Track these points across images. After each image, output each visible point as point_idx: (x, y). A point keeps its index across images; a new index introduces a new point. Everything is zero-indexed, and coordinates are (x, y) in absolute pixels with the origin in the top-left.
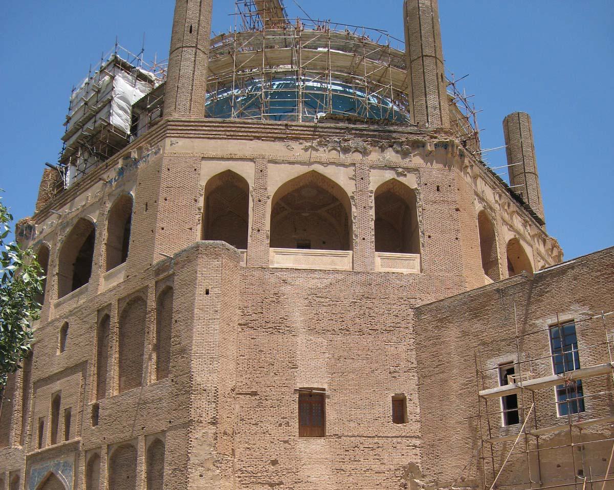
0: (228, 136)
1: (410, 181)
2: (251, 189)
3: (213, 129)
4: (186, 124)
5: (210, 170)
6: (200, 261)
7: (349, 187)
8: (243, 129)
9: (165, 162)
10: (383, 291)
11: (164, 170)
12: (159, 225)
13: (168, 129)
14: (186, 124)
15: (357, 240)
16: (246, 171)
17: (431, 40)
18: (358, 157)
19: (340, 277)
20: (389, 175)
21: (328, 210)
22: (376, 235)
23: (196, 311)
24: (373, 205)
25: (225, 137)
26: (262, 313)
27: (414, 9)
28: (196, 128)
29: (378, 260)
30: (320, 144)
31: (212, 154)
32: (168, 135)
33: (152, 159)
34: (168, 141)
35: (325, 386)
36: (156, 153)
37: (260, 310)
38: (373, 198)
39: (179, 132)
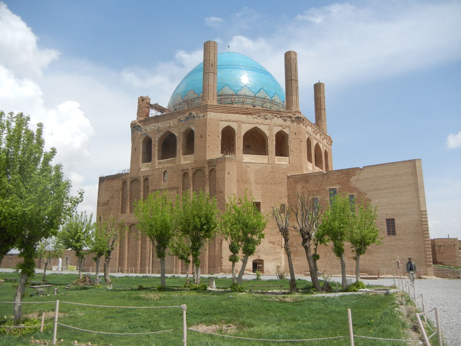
1: (286, 131)
6: (226, 163)
7: (267, 133)
9: (208, 122)
11: (208, 124)
12: (207, 145)
15: (270, 152)
16: (234, 126)
17: (295, 73)
19: (264, 165)
20: (280, 129)
23: (226, 180)
24: (275, 140)
29: (276, 159)
30: (258, 116)
31: (223, 119)
34: (208, 113)
35: (261, 201)
36: (204, 116)
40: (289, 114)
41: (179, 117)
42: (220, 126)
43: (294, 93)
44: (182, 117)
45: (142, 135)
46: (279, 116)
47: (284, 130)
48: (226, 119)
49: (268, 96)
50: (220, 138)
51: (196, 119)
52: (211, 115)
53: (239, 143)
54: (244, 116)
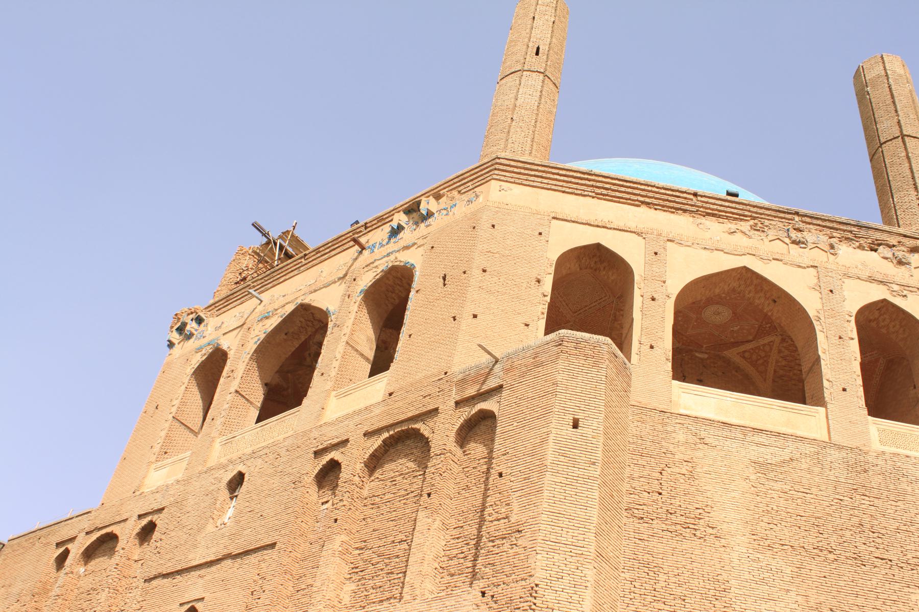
0: (597, 194)
2: (637, 278)
3: (573, 180)
4: (528, 166)
7: (810, 302)
8: (623, 189)
10: (892, 487)
13: (496, 169)
14: (528, 166)
15: (830, 390)
18: (818, 256)
19: (808, 449)
20: (876, 294)
21: (744, 352)
22: (864, 386)
25: (593, 194)
26: (660, 494)
27: (879, 76)
28: (544, 175)
30: (754, 228)
32: (495, 177)
37: (657, 488)
38: (853, 324)
39: (515, 175)
47: (898, 301)
53: (653, 323)
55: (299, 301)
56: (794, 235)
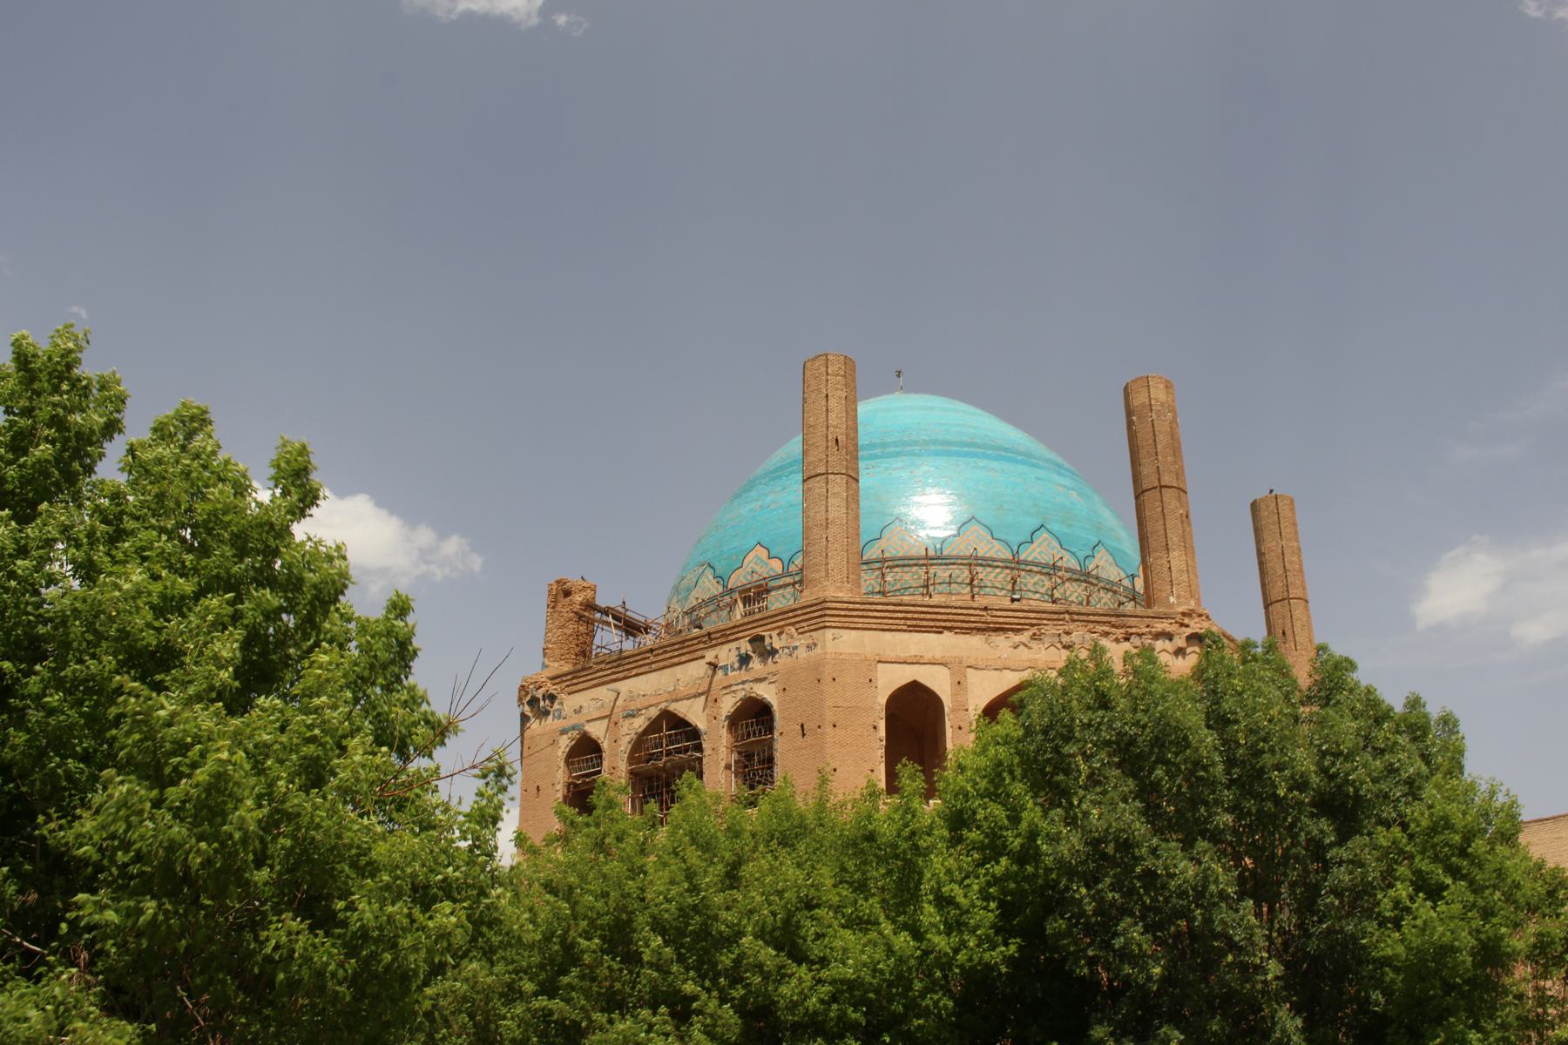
5: (892, 679)
16: (938, 681)
30: (1033, 637)
31: (891, 655)
33: (802, 653)
40: (1160, 626)
41: (710, 655)
42: (880, 683)
43: (1174, 539)
44: (726, 654)
45: (563, 732)
46: (1120, 633)
48: (903, 655)
49: (1067, 556)
50: (882, 732)
51: (782, 659)
52: (842, 643)
54: (976, 640)
55: (663, 706)
56: (1065, 639)
